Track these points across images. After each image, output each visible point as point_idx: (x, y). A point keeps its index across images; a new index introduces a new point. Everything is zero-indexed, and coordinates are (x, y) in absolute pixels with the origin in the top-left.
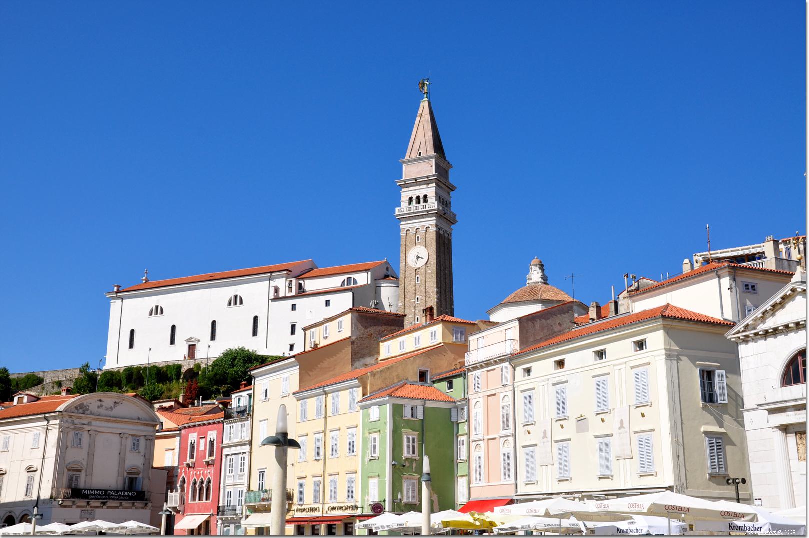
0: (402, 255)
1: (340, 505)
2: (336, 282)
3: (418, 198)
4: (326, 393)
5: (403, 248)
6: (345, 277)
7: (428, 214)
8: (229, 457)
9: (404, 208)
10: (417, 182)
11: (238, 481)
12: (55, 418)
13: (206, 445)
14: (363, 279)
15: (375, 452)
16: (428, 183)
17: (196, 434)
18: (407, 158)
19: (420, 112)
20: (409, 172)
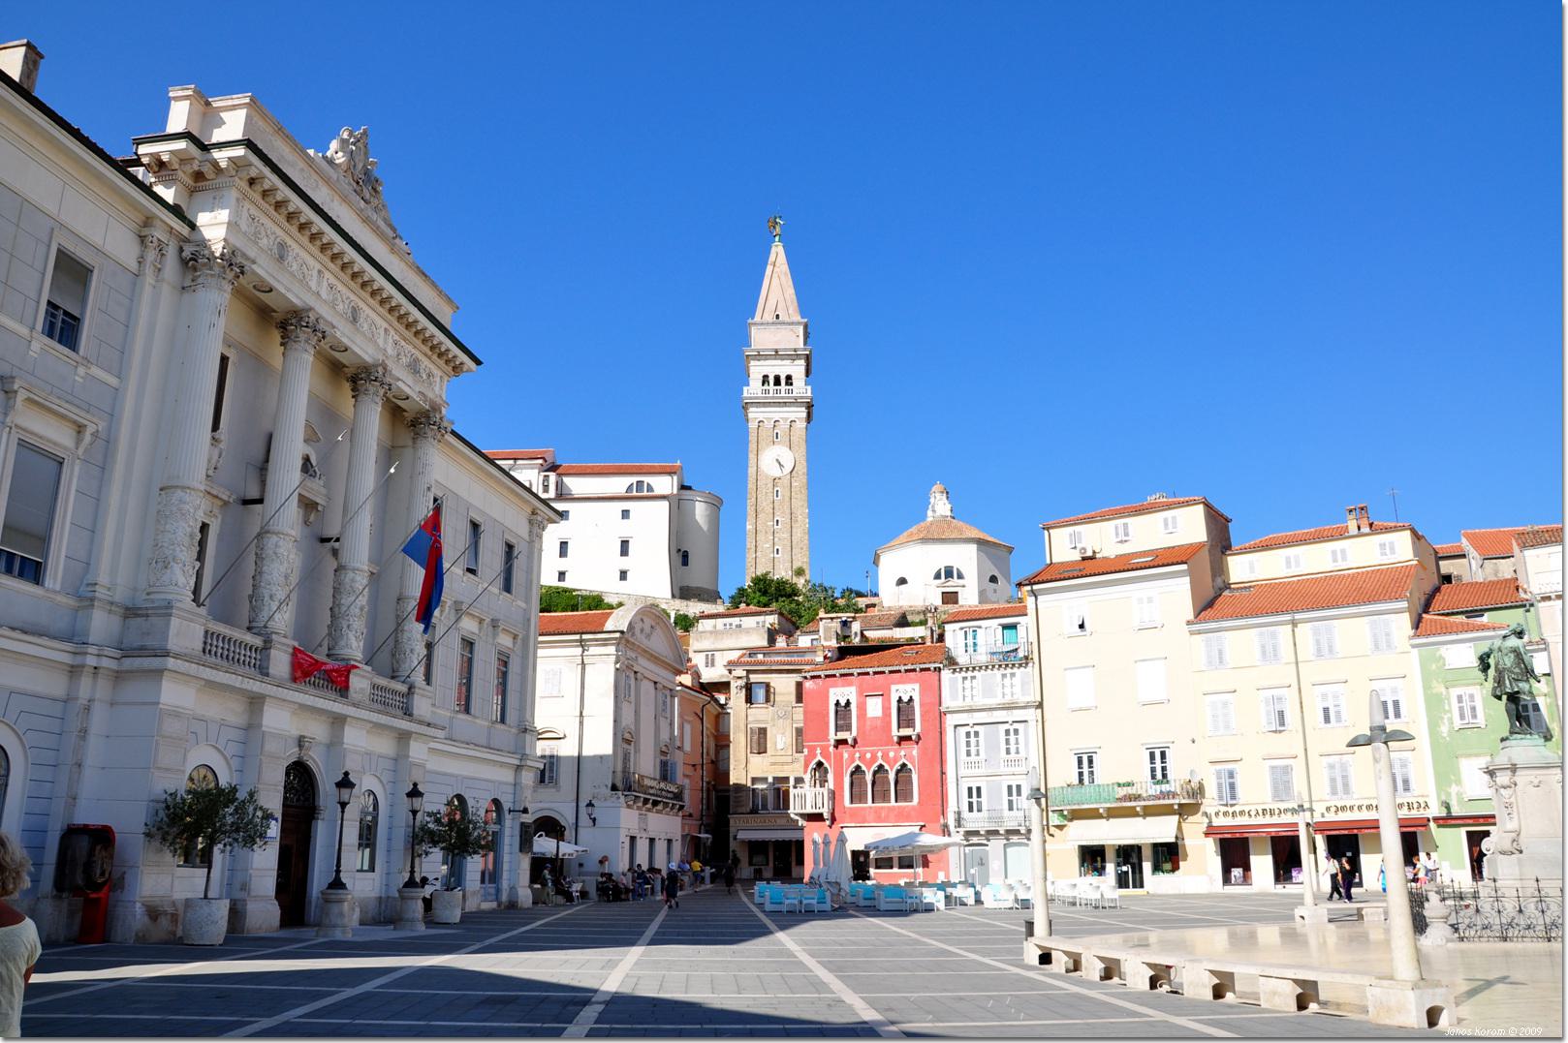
0: (752, 456)
1: (1366, 802)
2: (619, 484)
3: (777, 381)
4: (1294, 623)
5: (752, 446)
6: (634, 479)
7: (795, 403)
8: (962, 731)
9: (753, 389)
10: (776, 354)
11: (1003, 770)
12: (605, 643)
13: (886, 709)
14: (664, 485)
15: (1474, 716)
16: (794, 357)
17: (853, 689)
18: (757, 319)
19: (772, 258)
20: (761, 338)
